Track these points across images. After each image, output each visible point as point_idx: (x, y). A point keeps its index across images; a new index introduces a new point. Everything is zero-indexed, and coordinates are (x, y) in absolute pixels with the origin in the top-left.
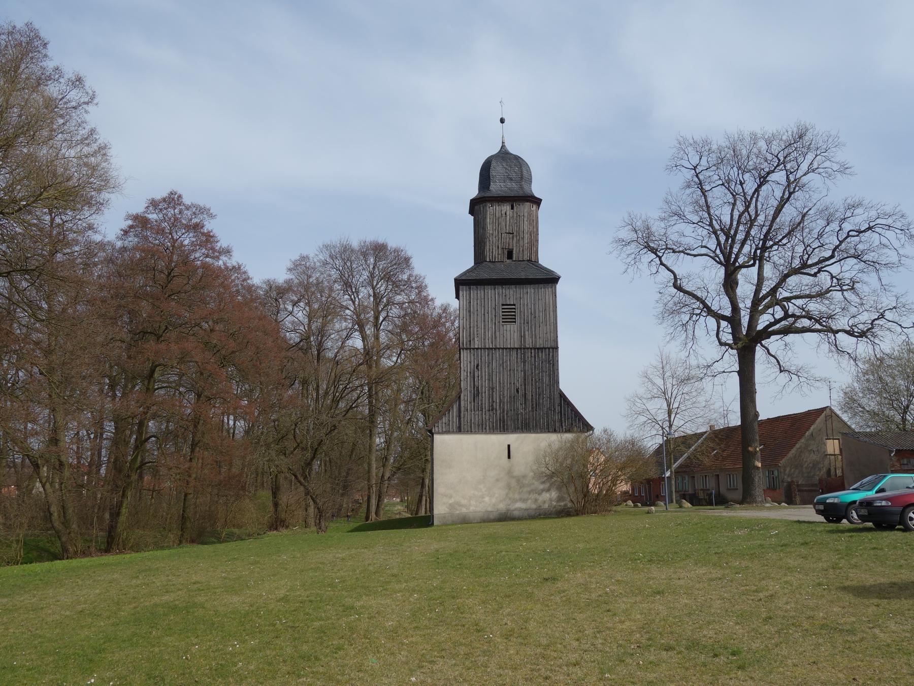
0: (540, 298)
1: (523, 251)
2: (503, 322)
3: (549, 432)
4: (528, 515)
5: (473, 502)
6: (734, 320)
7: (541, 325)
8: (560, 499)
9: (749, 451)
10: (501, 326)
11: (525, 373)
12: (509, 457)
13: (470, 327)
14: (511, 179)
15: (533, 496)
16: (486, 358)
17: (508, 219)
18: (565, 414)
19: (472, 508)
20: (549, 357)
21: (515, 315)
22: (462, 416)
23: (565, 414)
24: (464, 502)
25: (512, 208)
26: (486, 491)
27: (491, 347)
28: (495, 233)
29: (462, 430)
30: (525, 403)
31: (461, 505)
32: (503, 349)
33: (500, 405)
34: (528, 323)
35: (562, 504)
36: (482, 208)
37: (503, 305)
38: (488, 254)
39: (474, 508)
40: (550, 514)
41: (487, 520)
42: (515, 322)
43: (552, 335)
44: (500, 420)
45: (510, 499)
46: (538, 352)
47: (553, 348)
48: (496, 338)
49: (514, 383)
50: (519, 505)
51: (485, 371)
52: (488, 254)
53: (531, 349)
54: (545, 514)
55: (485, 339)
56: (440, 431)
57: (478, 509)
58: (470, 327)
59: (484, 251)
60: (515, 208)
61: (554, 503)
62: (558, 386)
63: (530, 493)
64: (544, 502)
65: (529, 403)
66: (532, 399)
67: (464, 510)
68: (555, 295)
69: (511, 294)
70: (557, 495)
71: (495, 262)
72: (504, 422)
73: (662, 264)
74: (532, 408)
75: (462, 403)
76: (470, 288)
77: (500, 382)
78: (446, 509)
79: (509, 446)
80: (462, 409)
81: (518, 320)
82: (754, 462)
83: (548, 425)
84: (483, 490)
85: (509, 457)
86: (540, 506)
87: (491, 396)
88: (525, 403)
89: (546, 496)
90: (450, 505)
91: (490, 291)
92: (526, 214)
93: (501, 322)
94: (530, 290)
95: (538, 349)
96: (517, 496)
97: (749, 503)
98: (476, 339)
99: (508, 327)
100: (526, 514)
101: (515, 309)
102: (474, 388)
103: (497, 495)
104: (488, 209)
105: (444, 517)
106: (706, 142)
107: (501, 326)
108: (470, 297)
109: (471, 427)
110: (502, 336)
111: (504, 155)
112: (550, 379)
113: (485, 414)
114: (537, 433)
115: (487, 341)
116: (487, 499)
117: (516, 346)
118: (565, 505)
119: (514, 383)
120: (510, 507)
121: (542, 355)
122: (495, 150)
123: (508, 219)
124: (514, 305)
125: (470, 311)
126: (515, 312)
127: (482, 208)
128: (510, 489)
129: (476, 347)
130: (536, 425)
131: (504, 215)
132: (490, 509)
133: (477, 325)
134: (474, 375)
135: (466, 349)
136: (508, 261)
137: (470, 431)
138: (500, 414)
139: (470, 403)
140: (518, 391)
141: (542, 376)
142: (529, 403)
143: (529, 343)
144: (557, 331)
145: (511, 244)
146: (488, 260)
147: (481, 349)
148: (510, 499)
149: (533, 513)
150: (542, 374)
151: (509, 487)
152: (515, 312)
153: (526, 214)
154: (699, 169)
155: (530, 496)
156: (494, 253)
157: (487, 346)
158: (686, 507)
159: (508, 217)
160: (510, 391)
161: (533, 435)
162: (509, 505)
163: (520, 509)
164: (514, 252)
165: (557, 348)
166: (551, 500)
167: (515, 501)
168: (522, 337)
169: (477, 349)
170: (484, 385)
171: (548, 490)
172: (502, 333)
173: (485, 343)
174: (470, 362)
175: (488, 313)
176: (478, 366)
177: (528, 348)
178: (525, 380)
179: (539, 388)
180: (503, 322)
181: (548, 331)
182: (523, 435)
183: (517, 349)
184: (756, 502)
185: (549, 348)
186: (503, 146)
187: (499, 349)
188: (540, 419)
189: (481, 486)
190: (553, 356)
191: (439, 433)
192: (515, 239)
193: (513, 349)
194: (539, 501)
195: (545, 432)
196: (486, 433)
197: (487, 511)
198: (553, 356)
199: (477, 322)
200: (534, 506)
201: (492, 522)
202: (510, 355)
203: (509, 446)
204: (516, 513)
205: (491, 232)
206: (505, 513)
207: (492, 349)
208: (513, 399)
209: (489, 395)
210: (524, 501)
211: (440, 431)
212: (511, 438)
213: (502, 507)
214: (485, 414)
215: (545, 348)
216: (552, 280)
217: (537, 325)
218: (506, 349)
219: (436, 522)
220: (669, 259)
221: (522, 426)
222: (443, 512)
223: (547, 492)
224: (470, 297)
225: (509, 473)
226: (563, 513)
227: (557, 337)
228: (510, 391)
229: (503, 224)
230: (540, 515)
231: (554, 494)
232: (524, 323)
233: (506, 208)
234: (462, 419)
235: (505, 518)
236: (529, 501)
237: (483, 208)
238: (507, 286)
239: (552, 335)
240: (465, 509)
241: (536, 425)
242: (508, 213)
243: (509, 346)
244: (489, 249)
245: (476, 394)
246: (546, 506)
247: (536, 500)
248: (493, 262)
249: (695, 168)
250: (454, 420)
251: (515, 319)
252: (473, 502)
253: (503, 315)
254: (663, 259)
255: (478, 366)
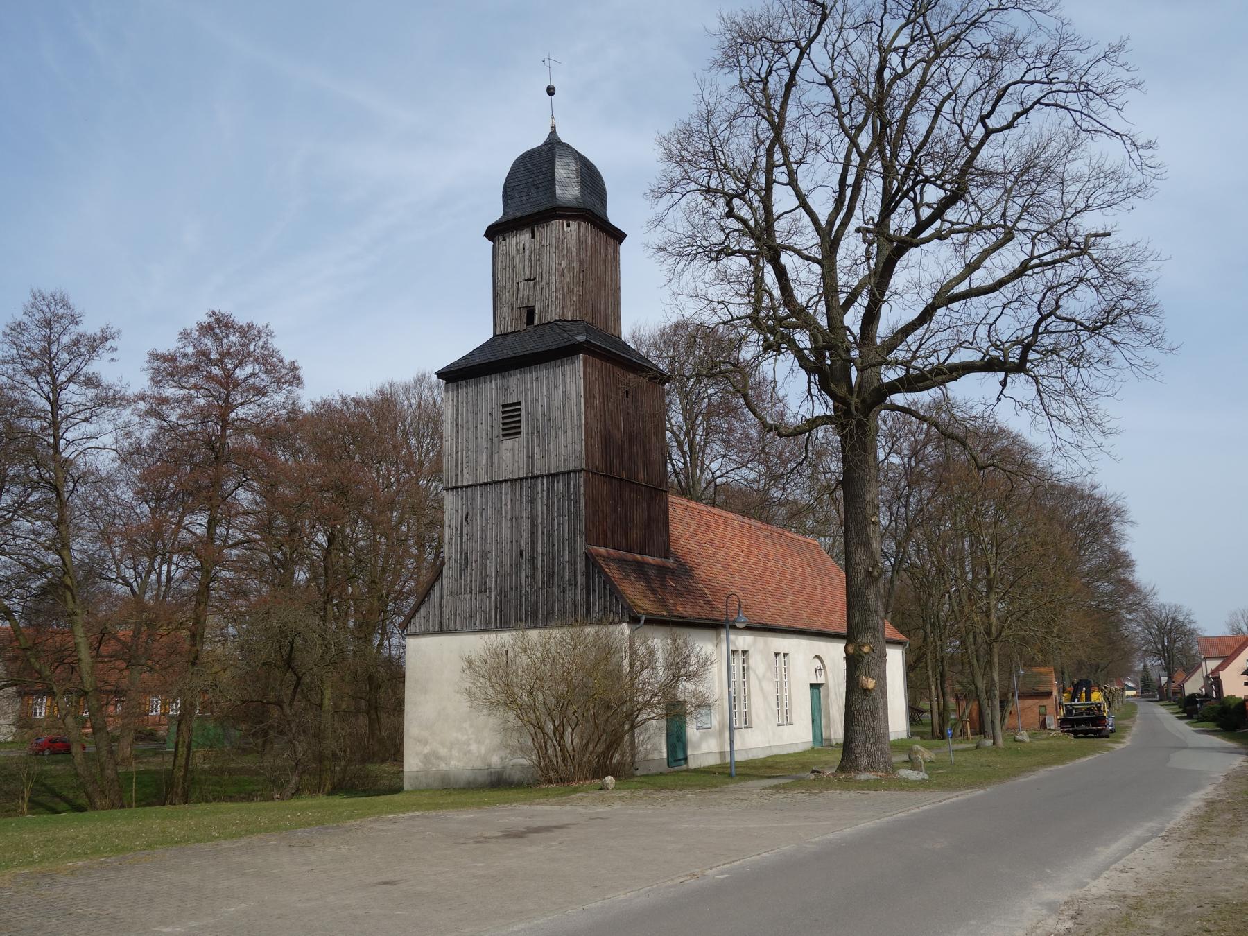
5: (455, 753)
11: (532, 521)
24: (443, 752)
31: (439, 758)
34: (538, 432)
44: (496, 607)
46: (553, 482)
51: (477, 522)
67: (443, 766)
72: (501, 611)
74: (543, 583)
78: (420, 764)
80: (446, 592)
81: (523, 429)
84: (470, 732)
87: (484, 566)
90: (426, 756)
95: (554, 475)
99: (512, 443)
102: (461, 554)
105: (417, 778)
111: (553, 147)
125: (457, 425)
131: (521, 251)
137: (455, 631)
140: (522, 555)
160: (511, 556)
164: (536, 311)
168: (531, 457)
176: (466, 517)
177: (537, 477)
178: (532, 533)
204: (517, 776)
209: (481, 565)
222: (415, 769)
228: (511, 556)
232: (533, 433)
240: (444, 765)
252: (455, 753)
255: (466, 517)
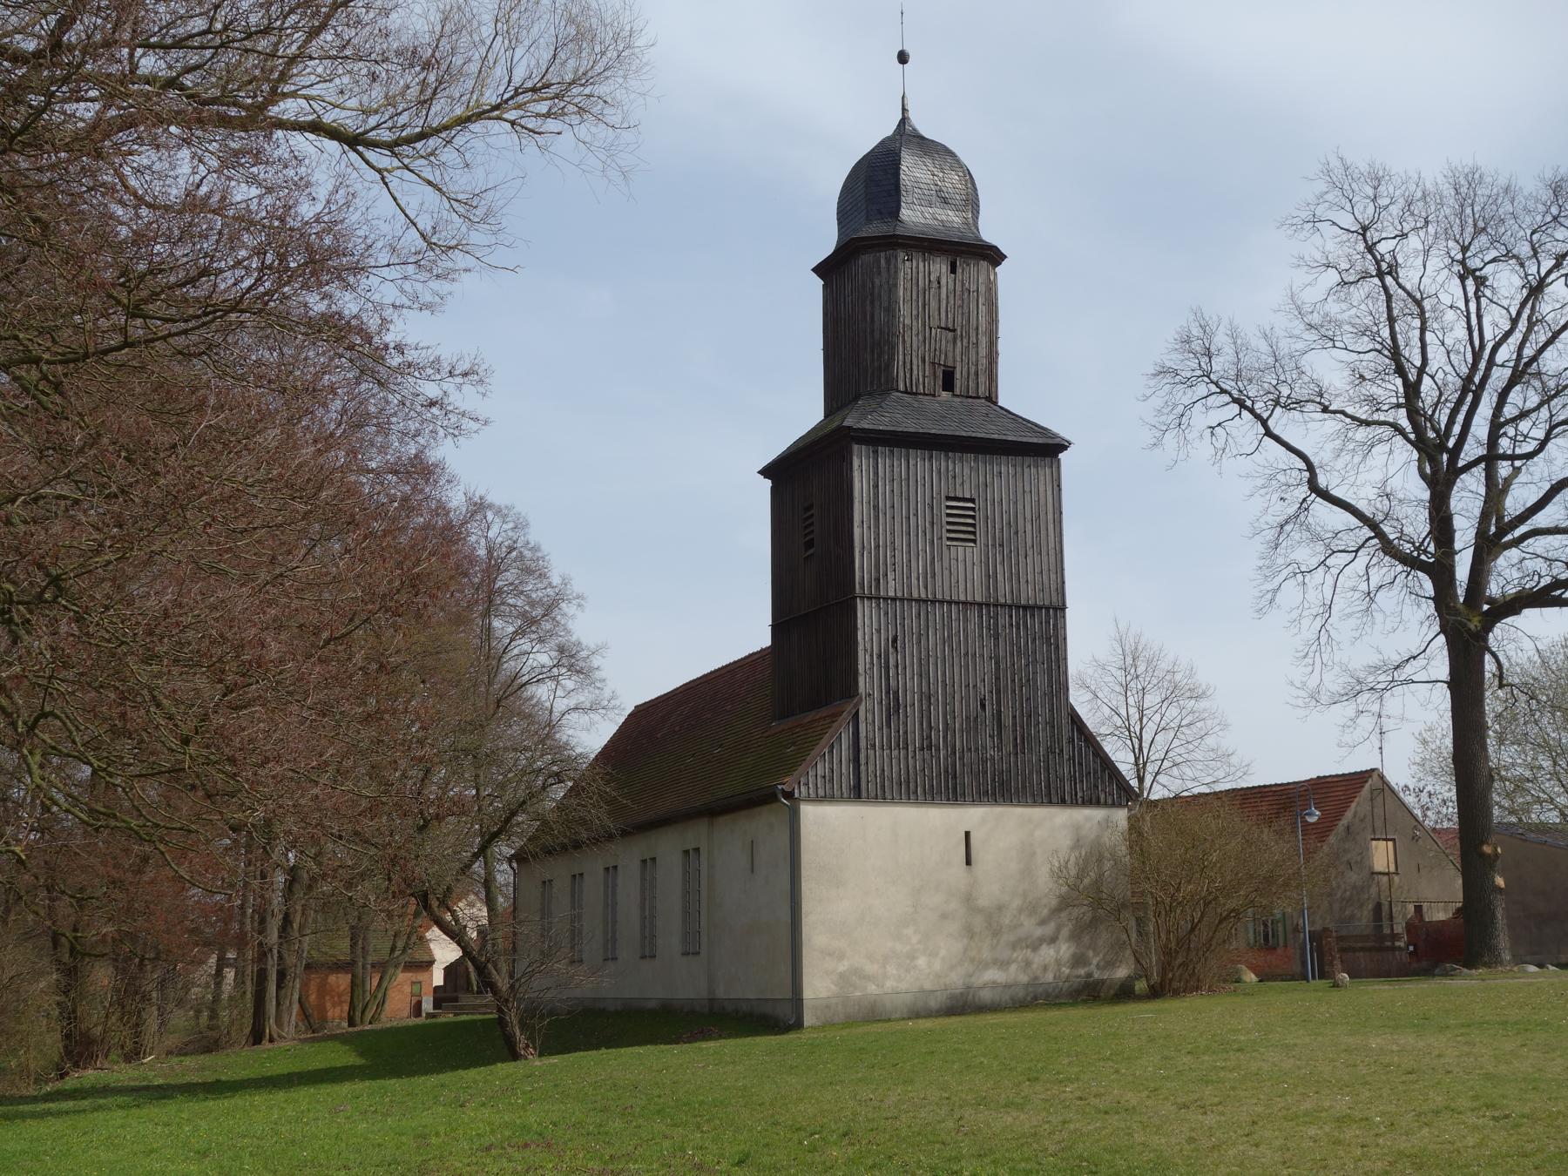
0: (1027, 489)
1: (977, 374)
2: (949, 539)
3: (1050, 803)
4: (1012, 999)
5: (891, 969)
6: (1441, 572)
7: (1030, 553)
8: (1078, 960)
9: (1482, 855)
10: (944, 548)
11: (997, 663)
12: (968, 862)
13: (877, 547)
14: (945, 201)
15: (1019, 955)
16: (912, 623)
17: (944, 296)
18: (1080, 764)
19: (890, 984)
20: (1048, 629)
21: (973, 525)
22: (863, 761)
23: (1080, 764)
24: (870, 968)
25: (953, 271)
26: (919, 942)
27: (923, 596)
28: (916, 326)
29: (864, 794)
30: (1000, 733)
31: (867, 978)
32: (950, 603)
33: (945, 737)
34: (1002, 545)
35: (1082, 972)
36: (883, 262)
37: (948, 498)
38: (901, 374)
39: (895, 984)
40: (1057, 997)
41: (916, 1014)
42: (974, 541)
43: (1053, 576)
44: (946, 771)
45: (972, 960)
46: (1025, 616)
47: (1055, 609)
48: (934, 576)
49: (975, 686)
50: (993, 975)
51: (911, 652)
52: (901, 374)
53: (1010, 607)
54: (1047, 996)
55: (909, 577)
56: (813, 795)
57: (903, 986)
58: (877, 547)
59: (889, 366)
60: (959, 270)
61: (1066, 971)
62: (1067, 699)
63: (1014, 946)
64: (1045, 968)
65: (1008, 735)
66: (1014, 724)
67: (872, 989)
68: (1059, 486)
69: (965, 474)
70: (1072, 950)
71: (916, 394)
72: (955, 777)
73: (1269, 433)
74: (1015, 746)
75: (862, 727)
76: (875, 452)
77: (944, 681)
78: (833, 987)
79: (967, 834)
80: (863, 744)
81: (981, 538)
82: (1494, 877)
83: (1048, 786)
84: (914, 940)
85: (968, 862)
86: (1036, 978)
87: (925, 715)
88: (1000, 733)
89: (1047, 954)
90: (841, 976)
91: (920, 465)
92: (982, 289)
93: (944, 539)
94: (1006, 467)
95: (1025, 608)
96: (986, 954)
97: (1487, 965)
98: (890, 576)
99: (960, 551)
100: (1006, 997)
101: (973, 509)
102: (888, 692)
103: (943, 953)
104: (900, 266)
105: (828, 1007)
106: (1466, 187)
107: (944, 548)
108: (876, 473)
109: (883, 787)
110: (946, 573)
111: (905, 136)
112: (1050, 681)
113: (914, 757)
114: (1026, 805)
115: (914, 581)
116: (921, 962)
117: (978, 599)
118: (1089, 975)
119: (975, 686)
120: (973, 979)
121: (1033, 622)
122: (889, 129)
123: (944, 296)
124: (972, 500)
125: (876, 507)
126: (973, 517)
127: (883, 262)
128: (972, 938)
129: (891, 594)
130: (1024, 787)
131: (935, 285)
132: (928, 986)
133: (893, 543)
134: (887, 662)
135: (870, 598)
136: (944, 394)
137: (881, 796)
138: (946, 759)
139: (881, 729)
140: (983, 706)
141: (1035, 673)
142: (1008, 735)
143: (1004, 593)
144: (1063, 569)
145: (950, 355)
146: (901, 387)
147: (902, 600)
148: (972, 960)
149: (1021, 994)
150: (1035, 667)
151: (969, 933)
152: (973, 517)
153: (982, 289)
154: (1373, 235)
155: (1015, 955)
156: (915, 372)
157: (915, 595)
158: (1248, 980)
159: (944, 290)
160: (968, 705)
161: (1018, 811)
162: (971, 976)
163: (994, 985)
164: (958, 375)
165: (1063, 608)
166: (1058, 962)
167: (985, 966)
168: (990, 577)
169: (894, 599)
170: (910, 685)
171: (1053, 940)
172: (946, 564)
173: (910, 587)
174: (879, 631)
175: (916, 515)
176: (895, 640)
177: (1002, 606)
178: (998, 679)
179: (1028, 699)
180: (949, 539)
181: (1045, 567)
182: (998, 810)
183: (980, 605)
184: (1501, 963)
185: (1048, 609)
186: (904, 121)
187: (942, 602)
188: (1031, 773)
189: (909, 931)
190: (1055, 625)
191: (809, 800)
192: (959, 344)
193: (971, 604)
194: (1035, 966)
195: (1042, 804)
196: (917, 803)
197: (922, 991)
198: (1055, 625)
199: (893, 533)
200: (1024, 978)
201: (936, 1017)
202: (966, 620)
203: (967, 834)
204: (986, 996)
205: (908, 322)
206: (962, 994)
207: (925, 601)
208: (972, 724)
209: (921, 711)
210: (1003, 965)
211: (813, 795)
212: (973, 816)
213: (956, 980)
214: (914, 757)
215: (1040, 608)
216: (1048, 449)
217: (1022, 552)
218: (957, 603)
219: (809, 1019)
220: (1281, 422)
221: (994, 788)
222: (824, 994)
223: (1049, 944)
224: (876, 473)
225: (968, 899)
226: (1090, 993)
227: (1063, 583)
228: (968, 705)
229: (934, 304)
230: (1035, 998)
231: (1065, 950)
232: (994, 545)
233: (939, 267)
234: (863, 768)
235: (961, 1006)
236: (1013, 967)
237: (888, 261)
238: (958, 455)
239: (1053, 576)
240: (874, 987)
241: (1024, 787)
242: (943, 281)
243: (962, 598)
244: (904, 363)
245: (894, 707)
246: (1049, 977)
247: (1028, 964)
248: (912, 393)
249: (1365, 229)
250: (843, 771)
251: (974, 533)
252: (891, 969)
253: (948, 523)
254: (1271, 423)
255: (895, 640)
